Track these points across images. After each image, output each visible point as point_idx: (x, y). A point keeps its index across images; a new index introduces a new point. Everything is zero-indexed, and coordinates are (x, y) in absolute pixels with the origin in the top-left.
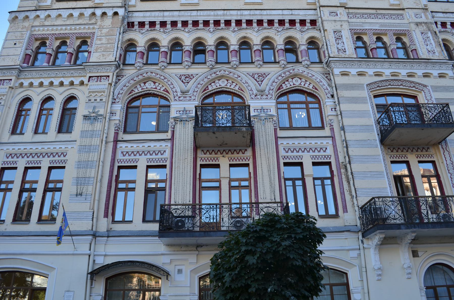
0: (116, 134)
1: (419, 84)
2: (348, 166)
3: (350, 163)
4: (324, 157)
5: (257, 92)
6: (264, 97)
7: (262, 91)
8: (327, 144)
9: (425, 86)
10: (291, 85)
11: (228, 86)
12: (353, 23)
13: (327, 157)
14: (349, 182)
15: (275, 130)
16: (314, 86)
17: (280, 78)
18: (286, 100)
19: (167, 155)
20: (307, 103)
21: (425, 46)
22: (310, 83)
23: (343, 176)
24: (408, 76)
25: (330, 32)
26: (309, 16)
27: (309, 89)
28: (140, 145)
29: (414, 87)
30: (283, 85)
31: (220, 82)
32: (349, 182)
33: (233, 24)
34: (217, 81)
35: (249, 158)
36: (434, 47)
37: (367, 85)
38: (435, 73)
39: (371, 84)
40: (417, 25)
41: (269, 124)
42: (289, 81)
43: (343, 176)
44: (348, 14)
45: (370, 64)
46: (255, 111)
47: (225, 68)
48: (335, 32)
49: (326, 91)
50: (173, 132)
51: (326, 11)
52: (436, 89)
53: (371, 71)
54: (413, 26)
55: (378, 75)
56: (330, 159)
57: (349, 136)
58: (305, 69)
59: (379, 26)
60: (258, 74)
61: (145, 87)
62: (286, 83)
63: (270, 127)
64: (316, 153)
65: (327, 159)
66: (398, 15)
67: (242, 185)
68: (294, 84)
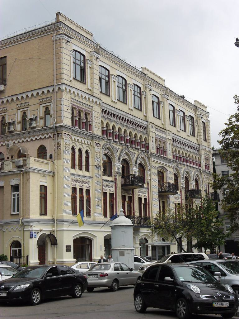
9: (168, 170)
19: (114, 189)
28: (108, 183)
50: (115, 179)
54: (168, 140)
55: (160, 163)
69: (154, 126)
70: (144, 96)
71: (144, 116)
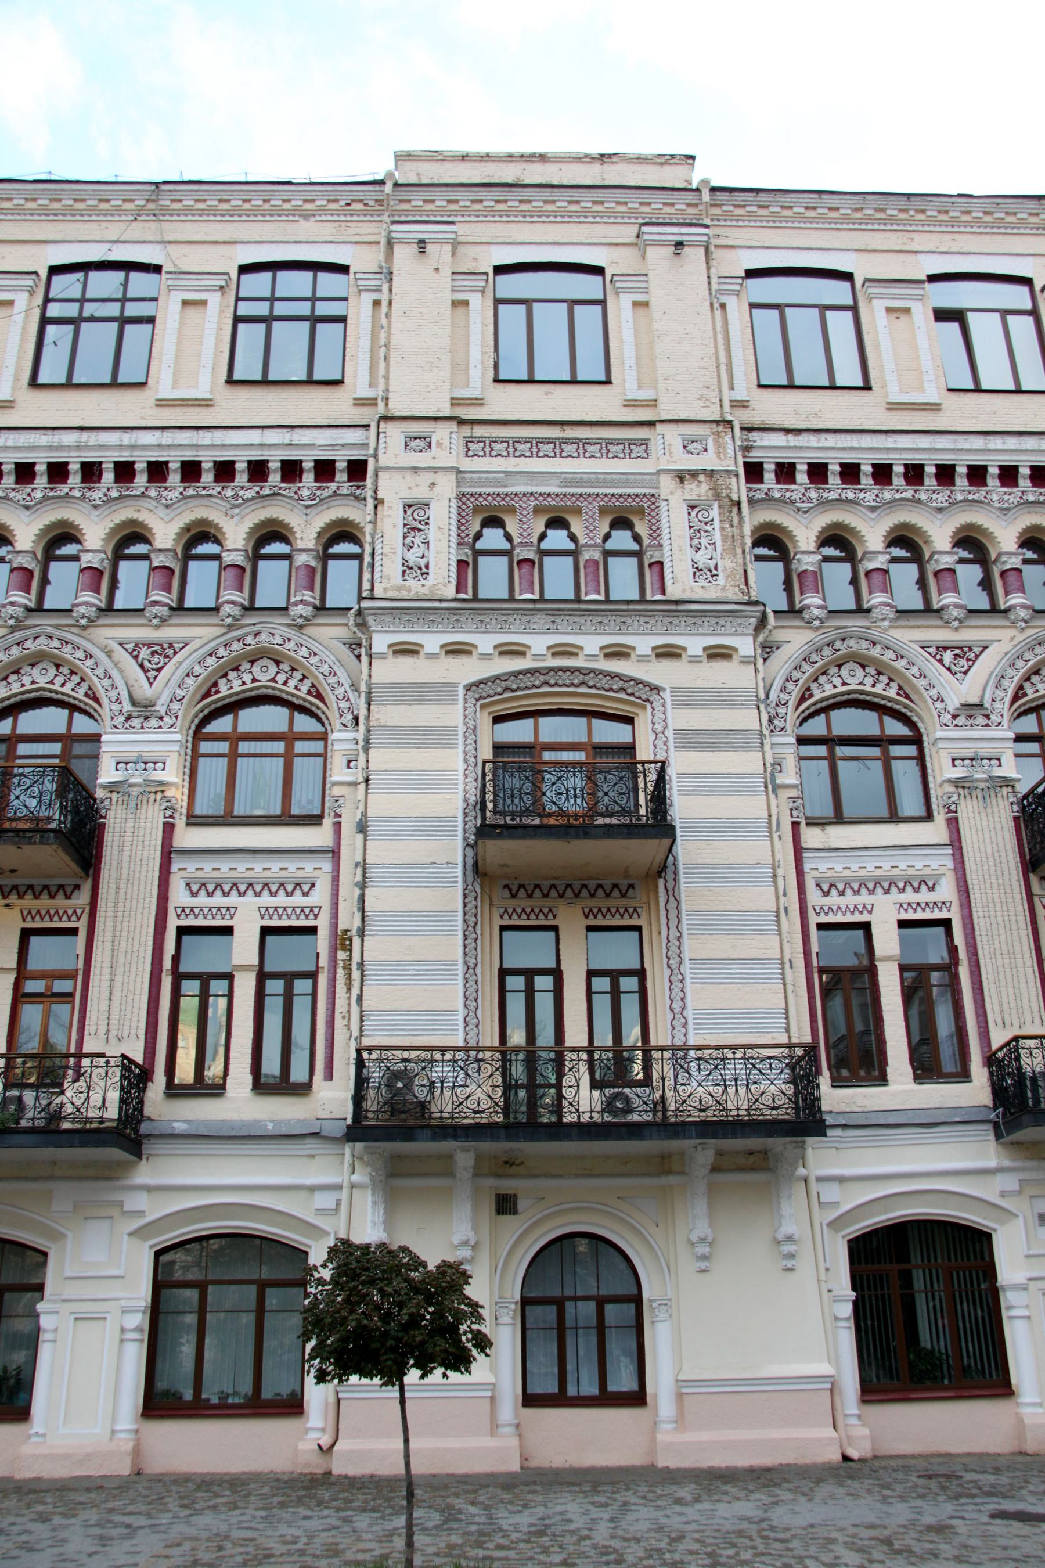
1: (638, 682)
2: (356, 941)
3: (362, 933)
4: (298, 911)
5: (130, 708)
6: (154, 722)
7: (146, 707)
8: (317, 873)
9: (656, 689)
10: (244, 683)
11: (56, 687)
12: (475, 476)
13: (307, 911)
14: (349, 989)
15: (169, 828)
16: (313, 686)
17: (211, 661)
18: (229, 729)
20: (289, 738)
21: (690, 553)
22: (304, 677)
23: (340, 972)
24: (607, 656)
25: (390, 508)
26: (339, 448)
27: (298, 697)
29: (622, 689)
30: (222, 682)
31: (35, 672)
32: (349, 989)
33: (108, 477)
34: (27, 669)
35: (79, 912)
36: (718, 555)
37: (469, 688)
38: (695, 645)
39: (481, 682)
40: (682, 480)
41: (151, 807)
42: (242, 668)
43: (340, 972)
44: (469, 441)
45: (487, 620)
46: (120, 766)
47: (50, 630)
48: (410, 506)
49: (344, 704)
51: (395, 433)
52: (688, 698)
53: (485, 642)
54: (667, 485)
56: (316, 916)
57: (378, 852)
58: (290, 633)
59: (557, 482)
60: (149, 646)
62: (232, 675)
63: (153, 818)
64: (281, 900)
65: (307, 916)
66: (632, 442)
67: (56, 990)
68: (254, 680)
69: (442, 433)
70: (367, 298)
71: (360, 402)
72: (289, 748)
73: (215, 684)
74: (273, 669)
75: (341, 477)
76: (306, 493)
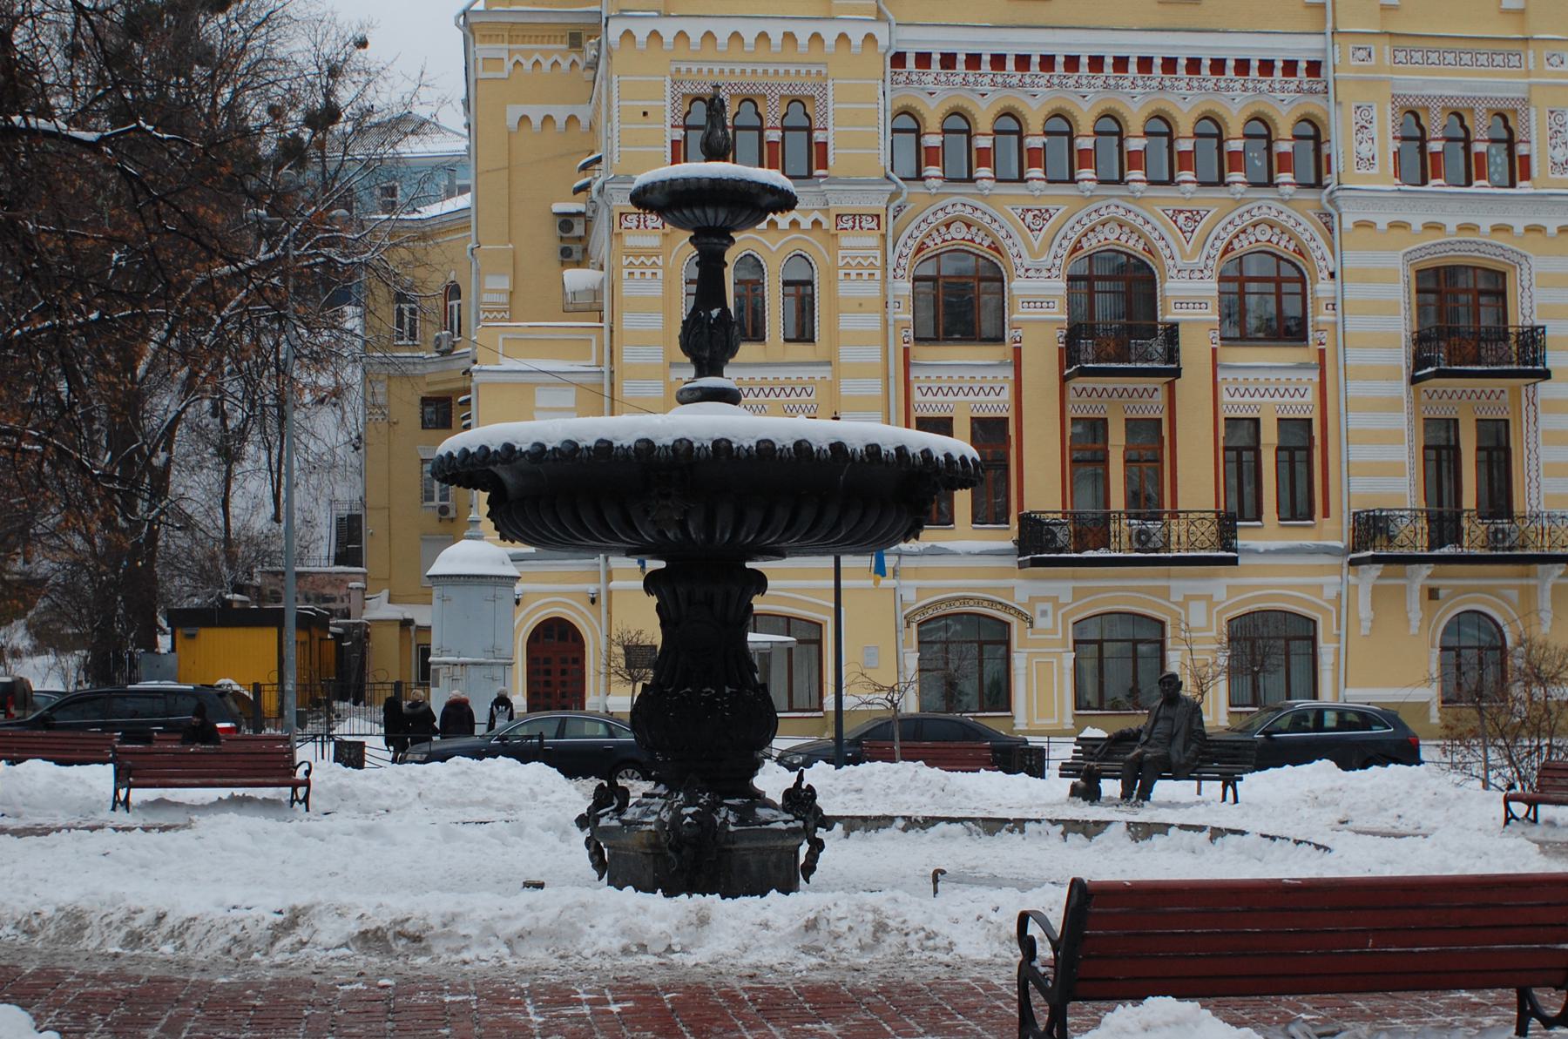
0: (906, 350)
15: (1214, 350)
33: (1133, 67)
49: (1322, 264)
61: (948, 237)
72: (1279, 288)
73: (1231, 243)
74: (1269, 232)
75: (1302, 73)
76: (1277, 86)
